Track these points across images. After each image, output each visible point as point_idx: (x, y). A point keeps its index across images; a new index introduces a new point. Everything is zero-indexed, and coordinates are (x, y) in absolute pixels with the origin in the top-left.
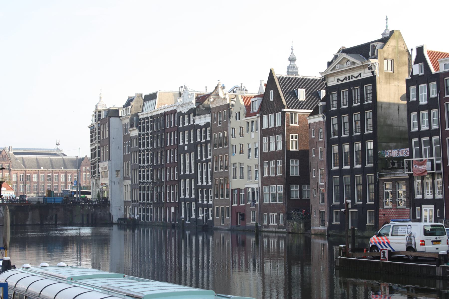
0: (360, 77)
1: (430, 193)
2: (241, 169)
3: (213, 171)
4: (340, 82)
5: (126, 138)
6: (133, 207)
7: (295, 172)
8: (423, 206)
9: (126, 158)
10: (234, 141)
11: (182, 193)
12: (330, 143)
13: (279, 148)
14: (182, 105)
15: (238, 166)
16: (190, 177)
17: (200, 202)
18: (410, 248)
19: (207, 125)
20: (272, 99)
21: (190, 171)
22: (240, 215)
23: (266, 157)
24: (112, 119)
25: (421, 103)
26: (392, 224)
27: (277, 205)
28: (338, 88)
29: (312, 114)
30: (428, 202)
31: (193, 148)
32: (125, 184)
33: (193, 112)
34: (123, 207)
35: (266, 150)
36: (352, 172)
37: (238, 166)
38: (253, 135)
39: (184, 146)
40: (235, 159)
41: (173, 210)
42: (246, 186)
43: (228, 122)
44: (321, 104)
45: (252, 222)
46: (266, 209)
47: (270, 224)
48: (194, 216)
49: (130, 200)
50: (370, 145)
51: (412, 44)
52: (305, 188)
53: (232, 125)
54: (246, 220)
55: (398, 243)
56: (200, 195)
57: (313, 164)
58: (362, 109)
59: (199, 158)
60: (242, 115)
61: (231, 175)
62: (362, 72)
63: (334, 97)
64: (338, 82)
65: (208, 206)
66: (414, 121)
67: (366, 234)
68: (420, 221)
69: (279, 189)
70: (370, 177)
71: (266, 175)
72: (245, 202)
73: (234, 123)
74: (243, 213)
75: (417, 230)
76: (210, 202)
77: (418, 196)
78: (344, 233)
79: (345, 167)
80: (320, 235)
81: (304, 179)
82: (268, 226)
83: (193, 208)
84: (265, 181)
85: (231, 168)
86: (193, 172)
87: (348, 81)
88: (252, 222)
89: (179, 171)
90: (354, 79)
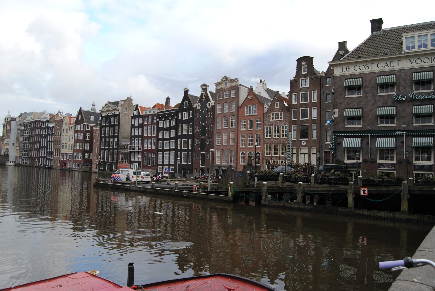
2: (66, 146)
3: (54, 146)
5: (18, 130)
7: (87, 148)
9: (18, 138)
10: (63, 134)
12: (101, 138)
13: (81, 138)
14: (44, 118)
15: (64, 144)
16: (44, 147)
18: (128, 179)
19: (53, 127)
20: (80, 119)
21: (45, 145)
22: (64, 163)
23: (76, 141)
24: (12, 122)
26: (121, 170)
27: (76, 160)
28: (106, 117)
29: (95, 126)
30: (136, 162)
31: (47, 136)
33: (47, 121)
35: (76, 139)
36: (109, 149)
37: (64, 144)
38: (71, 133)
39: (43, 135)
40: (63, 141)
43: (61, 127)
44: (99, 122)
46: (75, 162)
48: (45, 163)
49: (18, 155)
50: (116, 139)
51: (134, 103)
52: (91, 154)
53: (63, 128)
55: (123, 178)
57: (94, 145)
58: (114, 126)
60: (68, 124)
61: (61, 148)
62: (115, 112)
63: (104, 120)
65: (51, 160)
66: (133, 132)
67: (112, 173)
68: (132, 169)
69: (80, 154)
70: (115, 152)
71: (75, 148)
72: (66, 159)
73: (64, 127)
75: (131, 172)
77: (132, 160)
78: (104, 172)
79: (106, 147)
80: (95, 173)
81: (90, 151)
82: (75, 168)
84: (75, 151)
85: (62, 145)
89: (40, 145)
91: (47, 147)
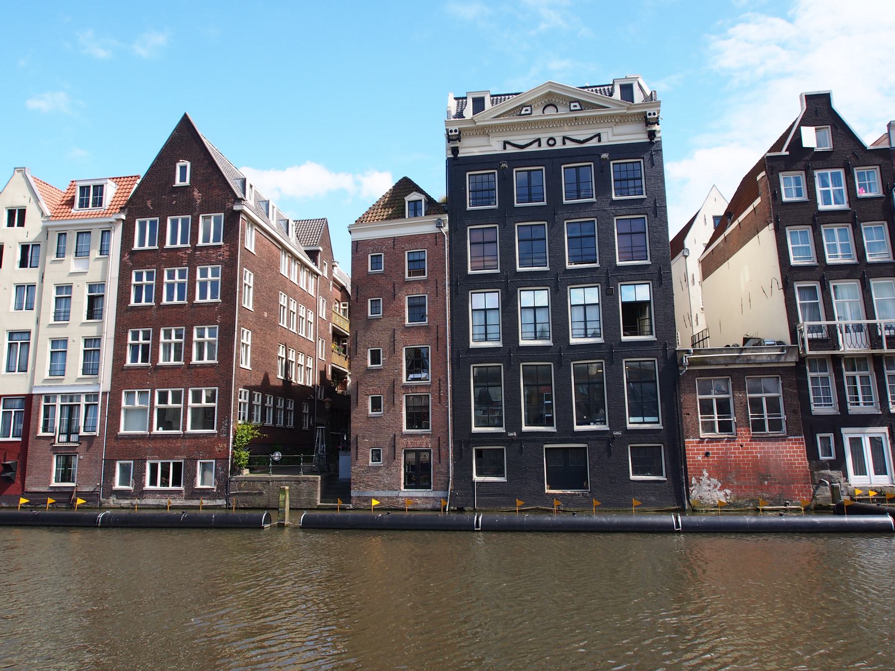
0: (599, 141)
1: (861, 401)
4: (510, 150)
8: (844, 430)
25: (822, 207)
64: (505, 148)
87: (545, 147)
90: (570, 145)
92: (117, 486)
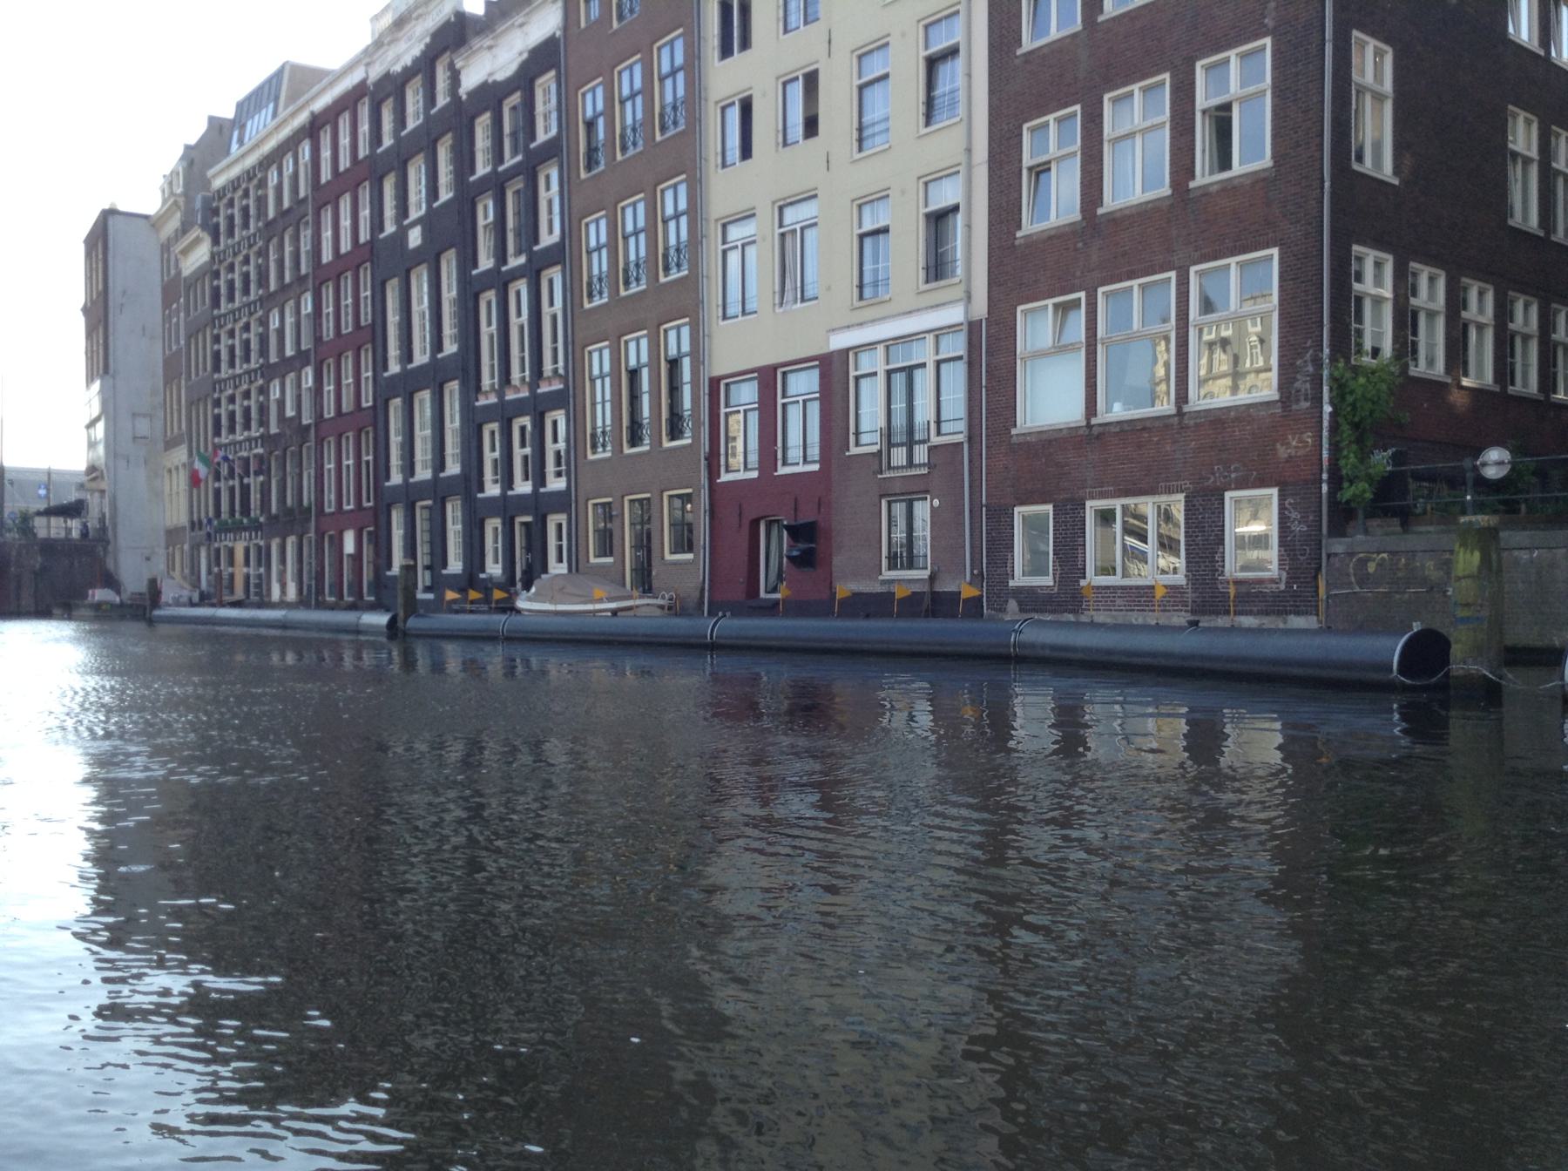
6: (195, 548)
11: (395, 460)
16: (435, 376)
17: (493, 490)
19: (544, 57)
31: (452, 228)
32: (169, 465)
34: (161, 551)
39: (402, 233)
41: (349, 546)
42: (838, 342)
45: (888, 575)
47: (1093, 579)
49: (183, 520)
54: (837, 561)
56: (490, 456)
59: (486, 263)
74: (806, 516)
76: (556, 484)
83: (454, 529)
86: (450, 348)
88: (888, 575)
89: (381, 362)
91: (467, 367)
92: (1019, 579)
